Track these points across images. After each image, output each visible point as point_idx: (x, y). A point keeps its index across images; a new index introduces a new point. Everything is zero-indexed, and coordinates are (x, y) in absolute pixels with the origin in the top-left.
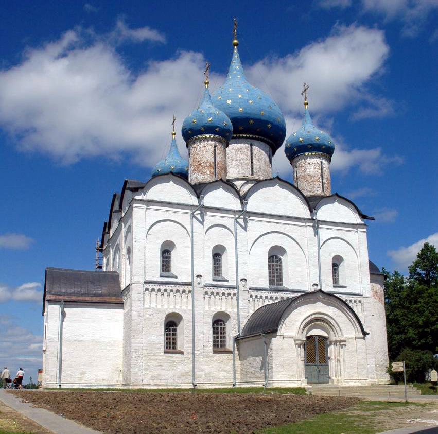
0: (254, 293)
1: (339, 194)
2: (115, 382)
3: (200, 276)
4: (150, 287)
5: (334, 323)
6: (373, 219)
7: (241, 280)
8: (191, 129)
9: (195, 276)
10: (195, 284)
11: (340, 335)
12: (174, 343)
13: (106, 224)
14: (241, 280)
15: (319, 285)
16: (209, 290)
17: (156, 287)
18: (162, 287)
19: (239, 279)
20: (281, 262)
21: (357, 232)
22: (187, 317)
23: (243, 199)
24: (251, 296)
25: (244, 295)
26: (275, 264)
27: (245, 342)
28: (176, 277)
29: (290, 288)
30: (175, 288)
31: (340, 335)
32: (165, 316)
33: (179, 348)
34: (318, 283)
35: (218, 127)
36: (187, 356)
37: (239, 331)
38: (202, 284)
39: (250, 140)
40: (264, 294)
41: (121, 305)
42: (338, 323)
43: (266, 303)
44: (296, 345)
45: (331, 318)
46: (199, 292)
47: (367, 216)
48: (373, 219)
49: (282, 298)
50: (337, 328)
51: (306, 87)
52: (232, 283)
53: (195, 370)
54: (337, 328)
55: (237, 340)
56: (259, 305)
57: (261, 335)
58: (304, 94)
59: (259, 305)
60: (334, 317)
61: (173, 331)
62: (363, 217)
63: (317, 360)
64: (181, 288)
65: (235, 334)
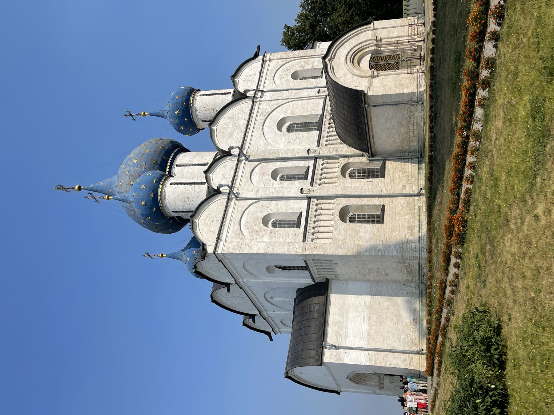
0: (323, 142)
1: (233, 74)
2: (418, 291)
3: (302, 189)
4: (309, 236)
5: (358, 47)
6: (259, 47)
7: (309, 154)
8: (151, 208)
9: (302, 195)
10: (309, 194)
11: (370, 42)
12: (373, 216)
13: (245, 325)
14: (308, 153)
15: (318, 89)
16: (317, 182)
17: (310, 231)
18: (311, 225)
19: (307, 155)
20: (295, 124)
21: (270, 60)
22: (344, 202)
23: (226, 154)
24: (326, 145)
25: (324, 151)
26: (295, 129)
27: (374, 142)
28: (301, 213)
29: (320, 112)
30: (312, 212)
31: (370, 42)
32: (342, 222)
33: (379, 212)
34: (317, 89)
35: (152, 180)
36: (387, 202)
37: (363, 156)
38: (310, 187)
39: (174, 166)
40: (325, 134)
41: (330, 283)
42: (358, 43)
43: (335, 133)
44: (378, 76)
45: (352, 49)
46: (317, 191)
47: (256, 52)
48: (259, 47)
49: (330, 119)
50: (363, 44)
51: (127, 114)
52: (311, 163)
53: (404, 192)
54: (363, 44)
55: (372, 154)
56: (336, 140)
57: (366, 110)
58: (135, 117)
59: (336, 140)
60: (352, 47)
61: (360, 218)
62: (256, 55)
63: (396, 61)
64: (313, 207)
65: (365, 159)
